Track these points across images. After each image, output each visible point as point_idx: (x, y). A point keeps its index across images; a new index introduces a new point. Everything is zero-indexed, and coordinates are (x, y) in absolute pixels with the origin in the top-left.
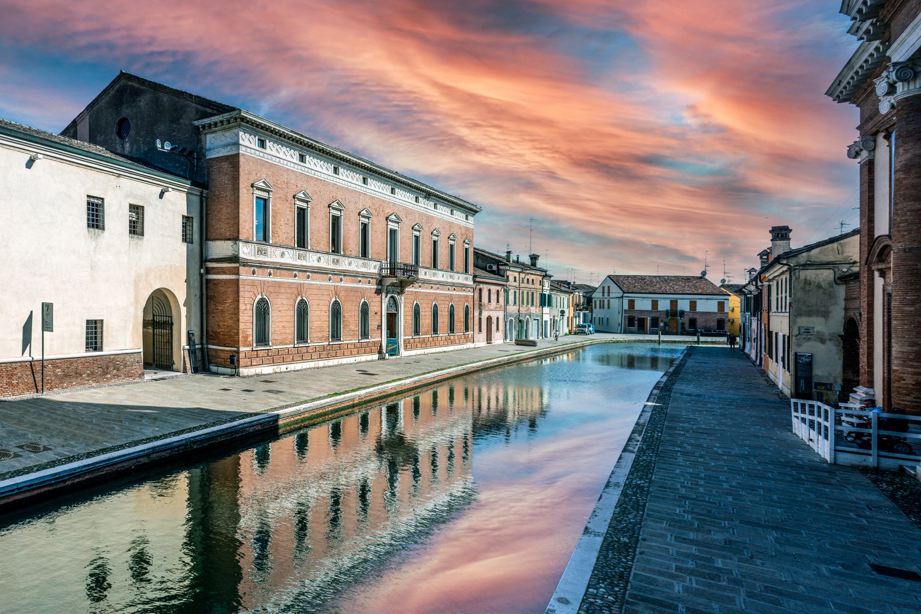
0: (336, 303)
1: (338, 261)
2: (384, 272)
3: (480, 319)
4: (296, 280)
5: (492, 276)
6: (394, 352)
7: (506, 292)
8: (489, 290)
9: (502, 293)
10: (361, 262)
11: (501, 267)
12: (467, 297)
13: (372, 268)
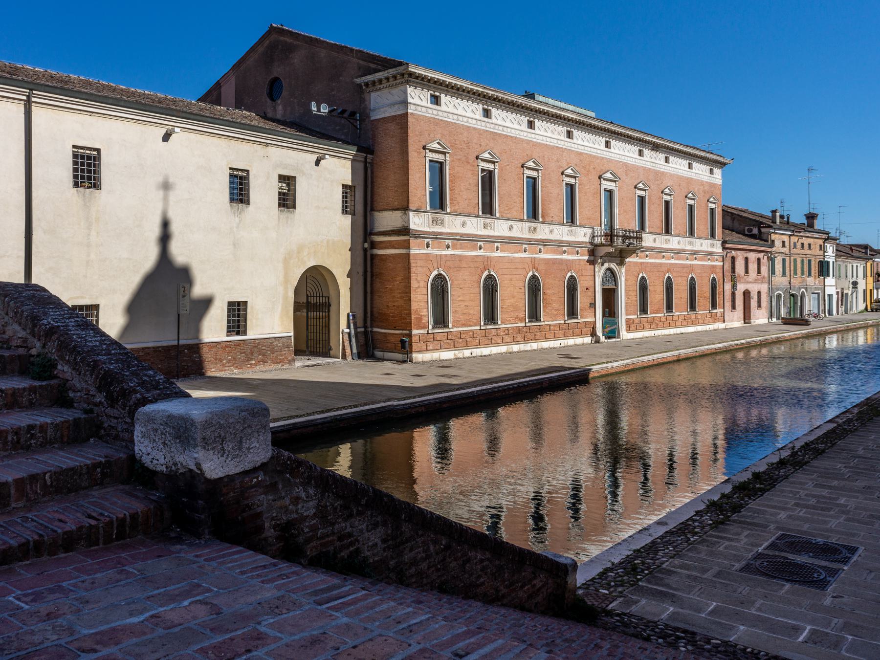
0: (534, 277)
1: (535, 229)
2: (597, 240)
3: (733, 294)
4: (481, 253)
5: (753, 240)
6: (612, 333)
7: (772, 260)
8: (746, 259)
9: (764, 261)
10: (566, 229)
11: (763, 230)
12: (713, 267)
13: (582, 235)
